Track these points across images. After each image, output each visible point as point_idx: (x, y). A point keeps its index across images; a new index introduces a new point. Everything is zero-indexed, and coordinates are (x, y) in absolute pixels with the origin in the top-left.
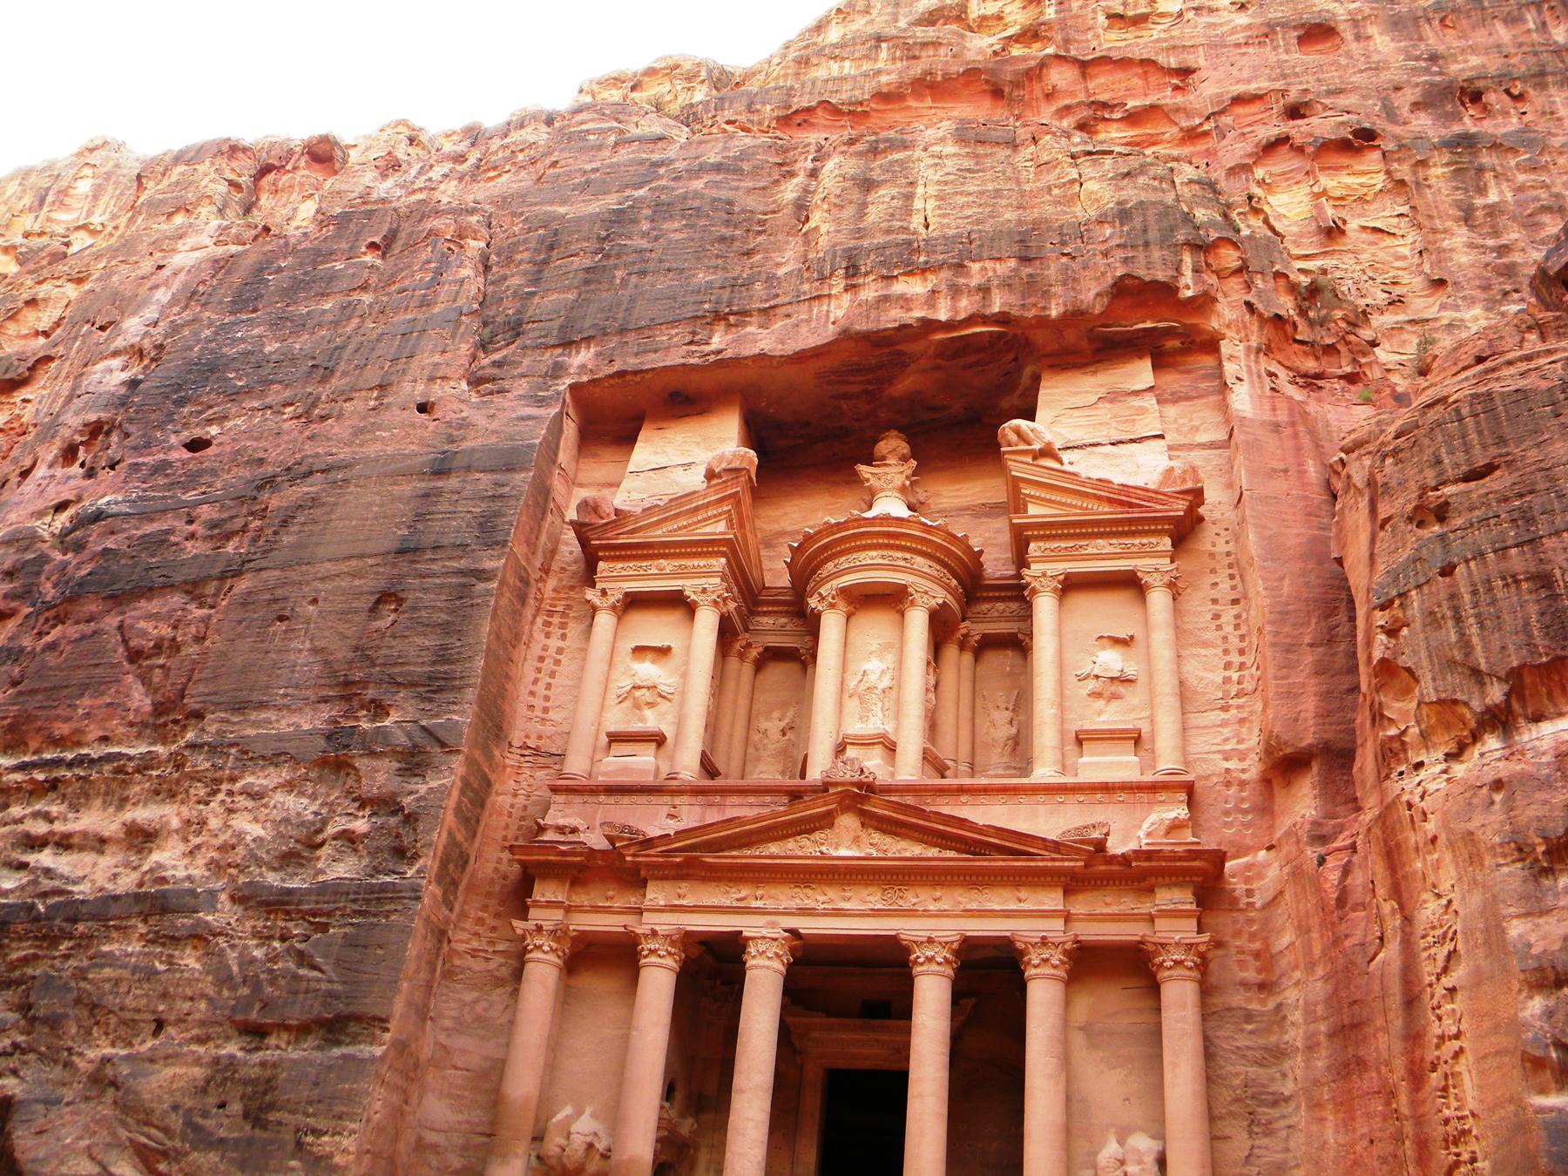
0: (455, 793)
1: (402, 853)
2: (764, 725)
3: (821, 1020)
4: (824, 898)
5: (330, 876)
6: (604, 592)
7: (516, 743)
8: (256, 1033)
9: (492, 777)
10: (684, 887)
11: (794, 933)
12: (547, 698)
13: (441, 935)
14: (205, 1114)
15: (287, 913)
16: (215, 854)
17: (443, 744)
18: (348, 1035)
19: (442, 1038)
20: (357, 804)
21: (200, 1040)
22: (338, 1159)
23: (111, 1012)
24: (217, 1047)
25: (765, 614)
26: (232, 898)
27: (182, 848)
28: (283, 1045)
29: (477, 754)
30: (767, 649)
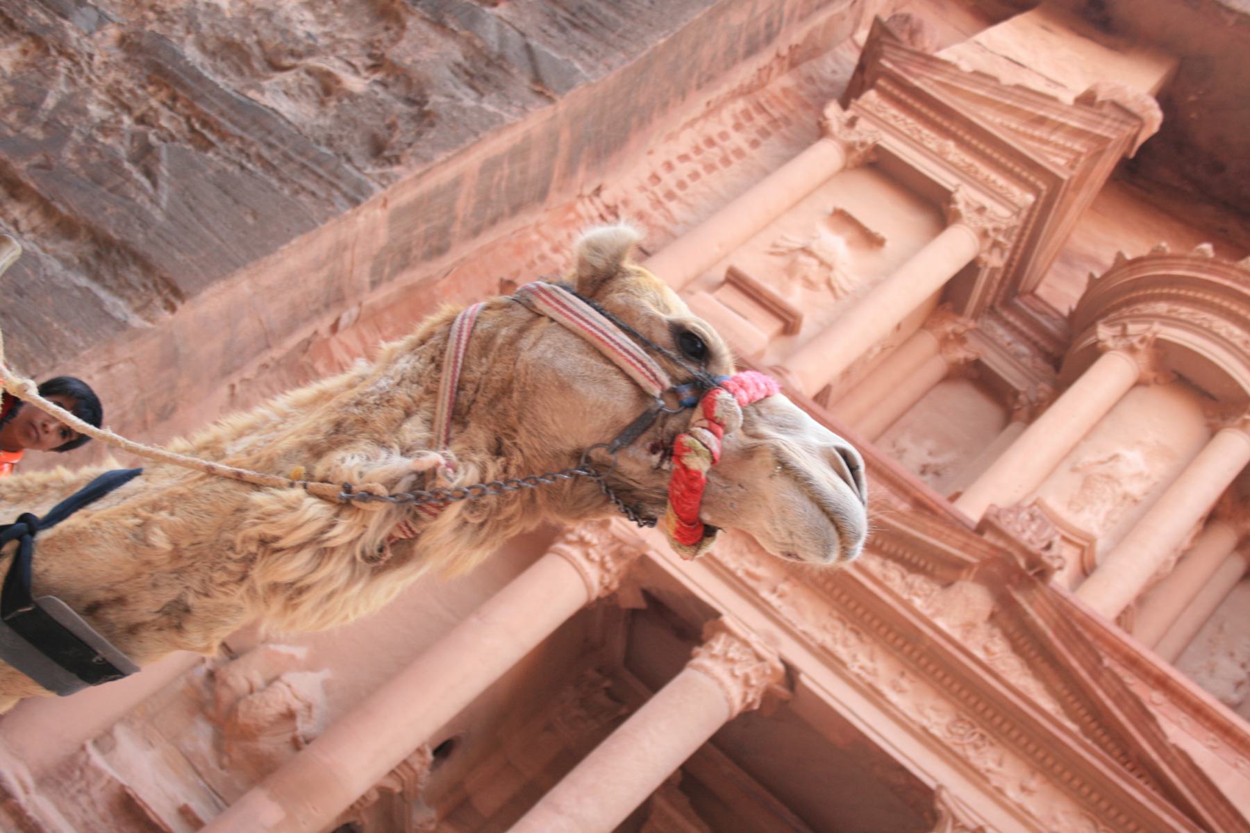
1: (379, 150)
2: (905, 442)
4: (868, 664)
5: (267, 100)
6: (852, 123)
7: (607, 196)
11: (791, 674)
12: (682, 185)
13: (336, 297)
15: (175, 98)
17: (537, 79)
18: (116, 276)
20: (369, 62)
25: (1006, 324)
29: (565, 136)
30: (977, 364)
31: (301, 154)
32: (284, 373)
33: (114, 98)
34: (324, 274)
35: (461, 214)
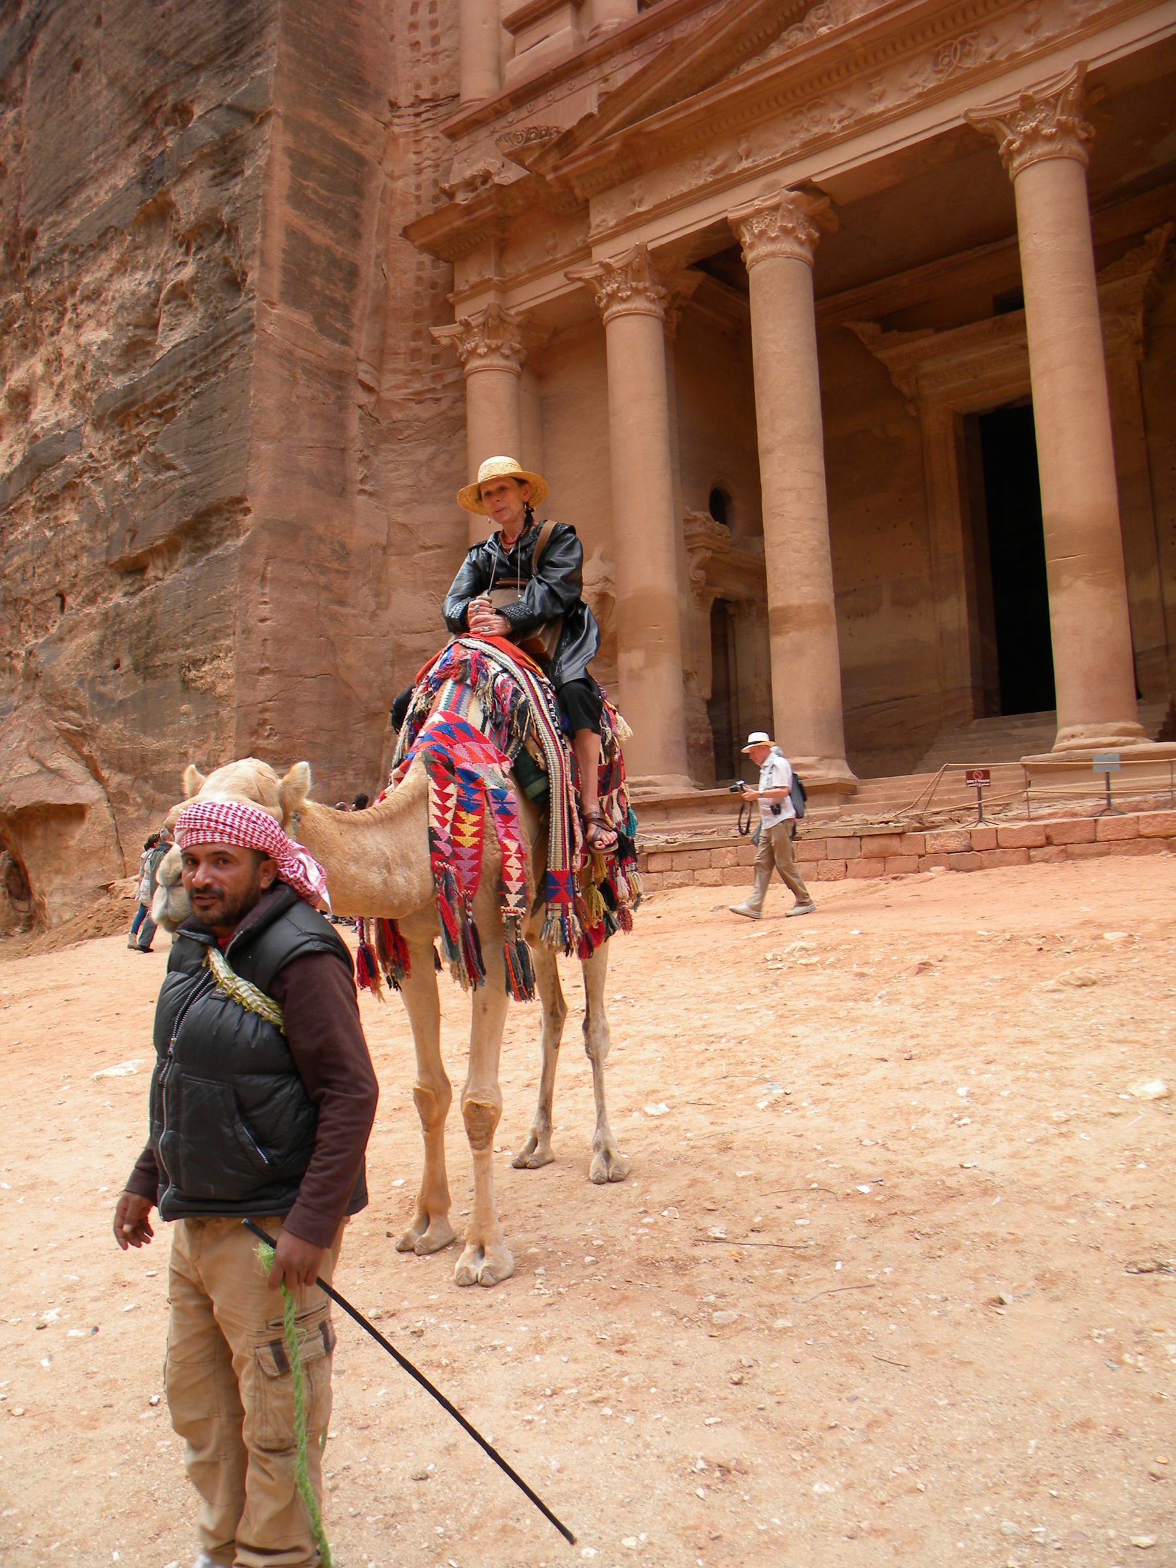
0: (282, 176)
3: (927, 340)
7: (404, 100)
8: (134, 569)
9: (368, 151)
10: (637, 188)
11: (804, 186)
14: (104, 680)
15: (137, 415)
16: (75, 386)
18: (213, 534)
19: (400, 517)
21: (91, 600)
22: (221, 689)
23: (27, 602)
24: (105, 600)
26: (97, 425)
27: (51, 394)
28: (160, 575)
29: (312, 116)
31: (207, 346)
32: (383, 446)
33: (120, 458)
34: (302, 379)
35: (328, 242)
